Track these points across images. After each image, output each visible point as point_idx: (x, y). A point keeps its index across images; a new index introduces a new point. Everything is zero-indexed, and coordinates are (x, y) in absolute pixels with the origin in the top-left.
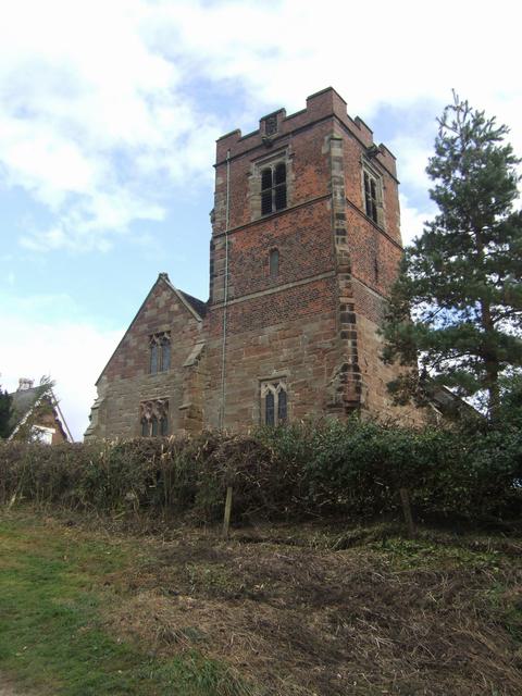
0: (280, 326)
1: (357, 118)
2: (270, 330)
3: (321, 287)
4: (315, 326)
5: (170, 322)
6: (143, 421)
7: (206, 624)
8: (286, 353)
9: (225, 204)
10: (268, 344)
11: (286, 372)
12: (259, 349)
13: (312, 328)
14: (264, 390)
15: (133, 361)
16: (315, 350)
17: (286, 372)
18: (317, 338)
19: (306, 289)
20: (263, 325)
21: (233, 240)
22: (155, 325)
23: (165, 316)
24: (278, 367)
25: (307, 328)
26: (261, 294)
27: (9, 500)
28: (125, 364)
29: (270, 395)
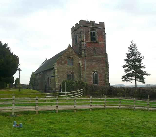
0: (96, 63)
1: (100, 22)
2: (94, 63)
3: (103, 58)
4: (102, 64)
5: (73, 56)
6: (68, 75)
7: (43, 133)
8: (97, 68)
9: (84, 35)
10: (94, 65)
11: (97, 71)
12: (92, 66)
13: (102, 65)
14: (93, 73)
15: (64, 62)
16: (102, 68)
17: (97, 71)
18: (102, 67)
19: (101, 58)
20: (93, 62)
21: (86, 43)
22: (69, 55)
23: (71, 54)
24: (96, 70)
25: (101, 64)
26: (92, 56)
27: (96, 85)
28: (62, 62)
29: (94, 74)
